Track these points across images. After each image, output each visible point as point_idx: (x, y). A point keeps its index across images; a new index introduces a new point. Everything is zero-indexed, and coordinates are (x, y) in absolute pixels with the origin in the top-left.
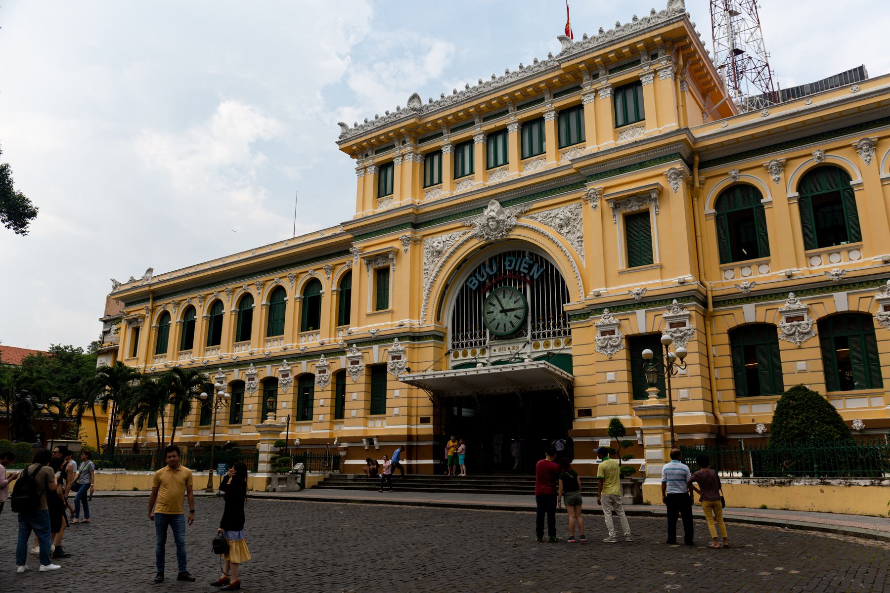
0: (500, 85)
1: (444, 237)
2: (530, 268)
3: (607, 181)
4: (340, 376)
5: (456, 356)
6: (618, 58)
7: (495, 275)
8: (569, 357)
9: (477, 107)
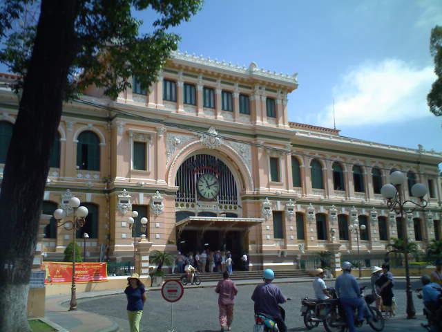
5: (177, 205)
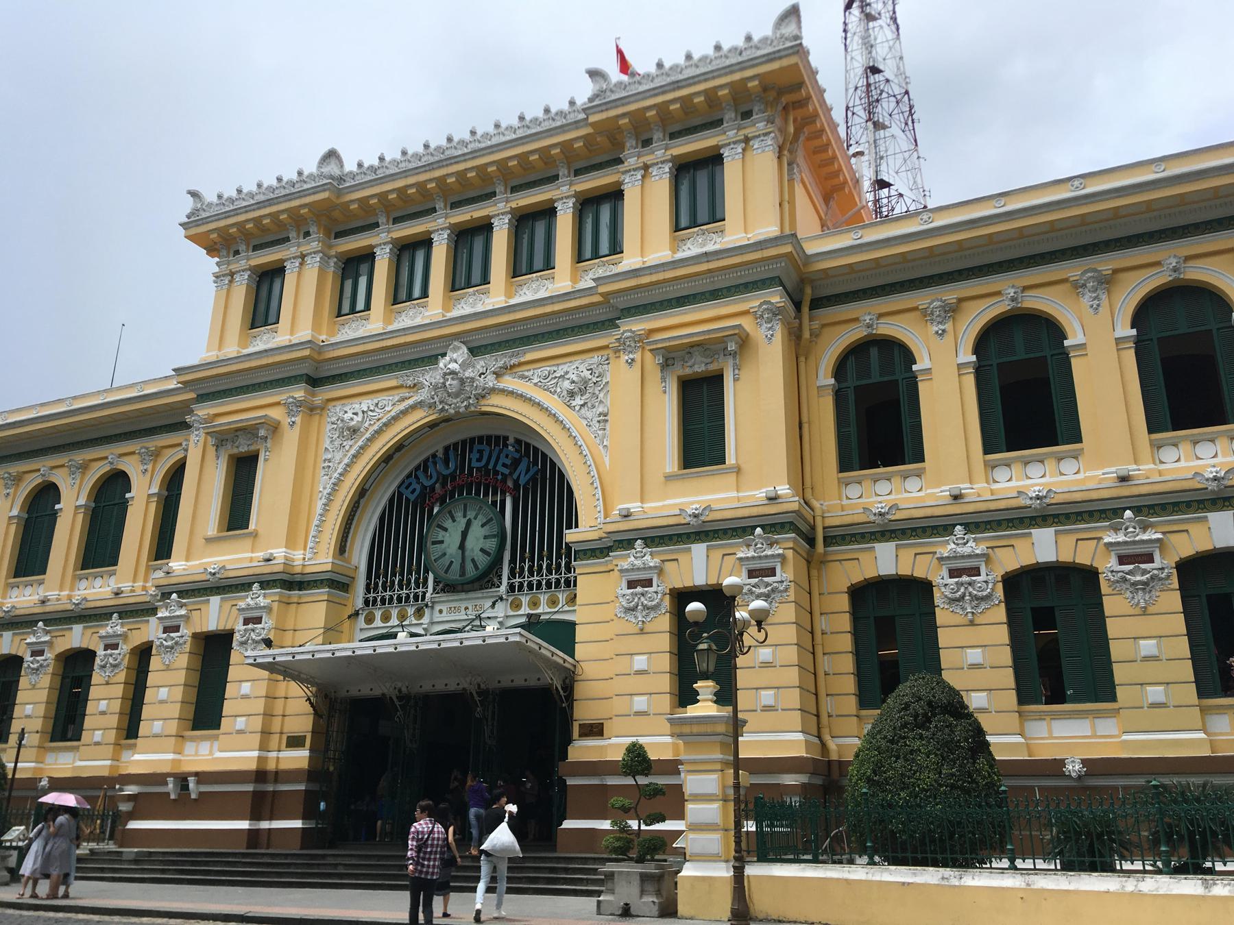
0: (483, 145)
1: (366, 404)
2: (516, 463)
3: (655, 318)
4: (143, 654)
6: (686, 114)
7: (453, 476)
8: (572, 625)
9: (441, 180)
